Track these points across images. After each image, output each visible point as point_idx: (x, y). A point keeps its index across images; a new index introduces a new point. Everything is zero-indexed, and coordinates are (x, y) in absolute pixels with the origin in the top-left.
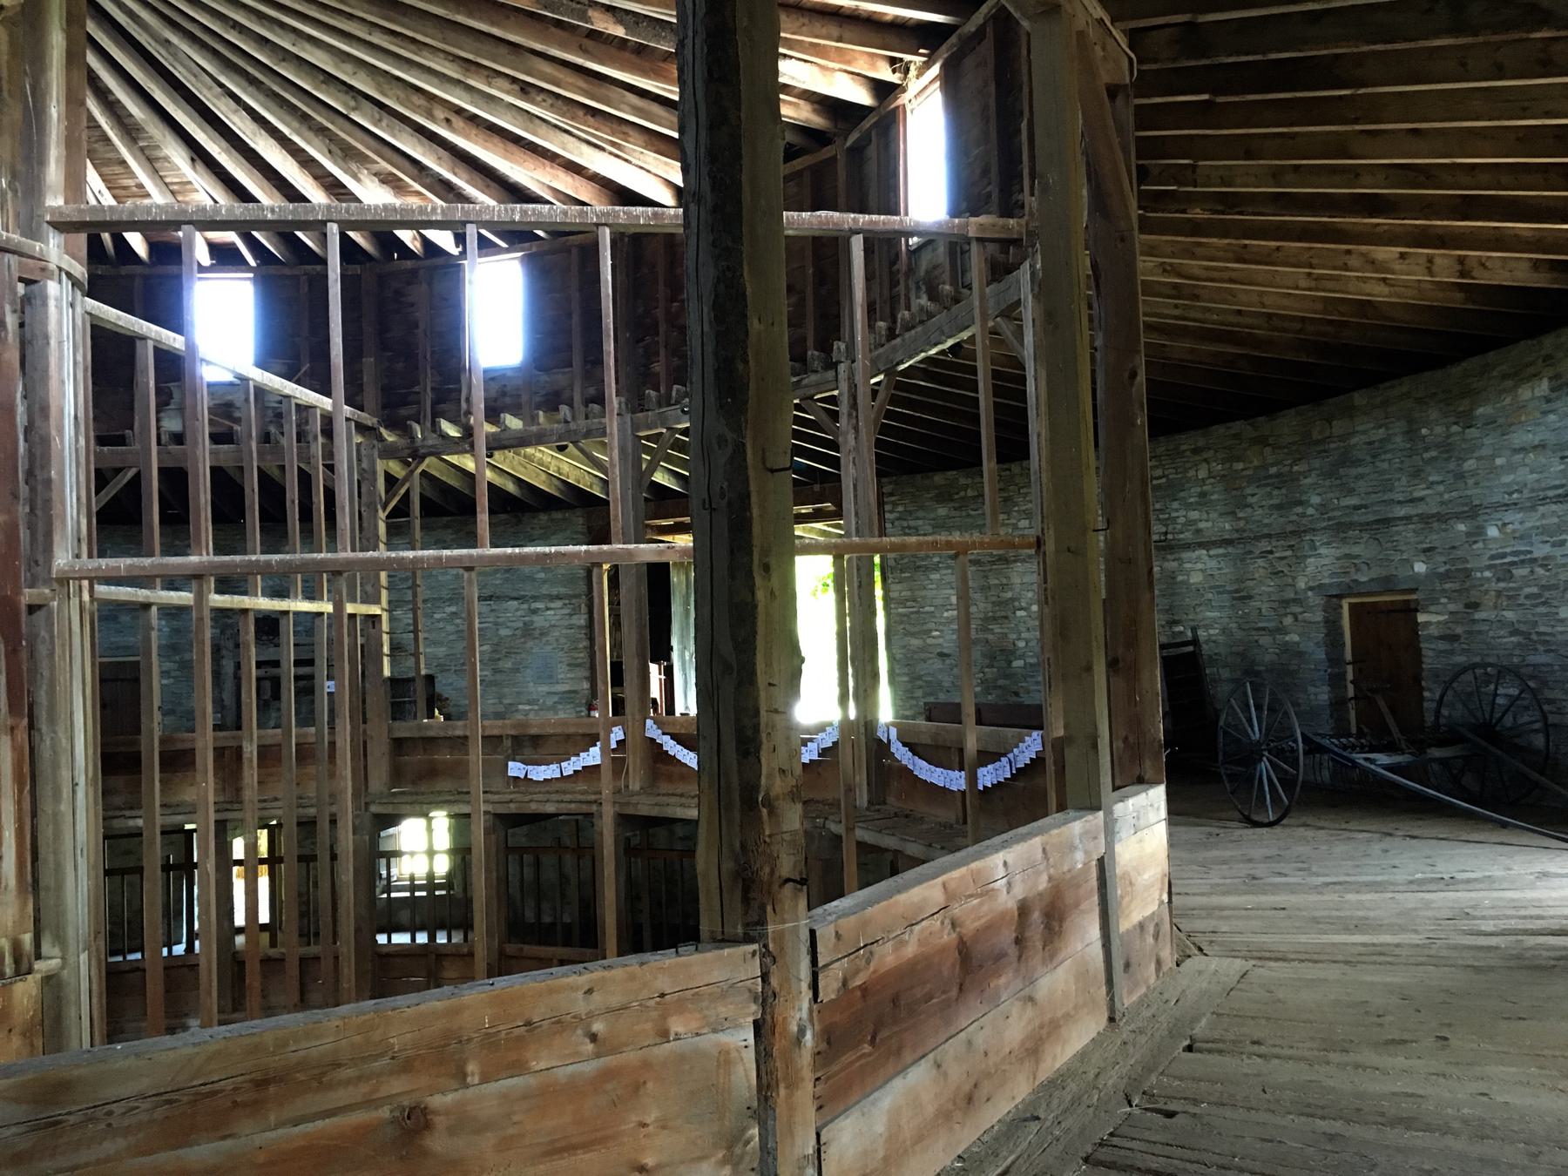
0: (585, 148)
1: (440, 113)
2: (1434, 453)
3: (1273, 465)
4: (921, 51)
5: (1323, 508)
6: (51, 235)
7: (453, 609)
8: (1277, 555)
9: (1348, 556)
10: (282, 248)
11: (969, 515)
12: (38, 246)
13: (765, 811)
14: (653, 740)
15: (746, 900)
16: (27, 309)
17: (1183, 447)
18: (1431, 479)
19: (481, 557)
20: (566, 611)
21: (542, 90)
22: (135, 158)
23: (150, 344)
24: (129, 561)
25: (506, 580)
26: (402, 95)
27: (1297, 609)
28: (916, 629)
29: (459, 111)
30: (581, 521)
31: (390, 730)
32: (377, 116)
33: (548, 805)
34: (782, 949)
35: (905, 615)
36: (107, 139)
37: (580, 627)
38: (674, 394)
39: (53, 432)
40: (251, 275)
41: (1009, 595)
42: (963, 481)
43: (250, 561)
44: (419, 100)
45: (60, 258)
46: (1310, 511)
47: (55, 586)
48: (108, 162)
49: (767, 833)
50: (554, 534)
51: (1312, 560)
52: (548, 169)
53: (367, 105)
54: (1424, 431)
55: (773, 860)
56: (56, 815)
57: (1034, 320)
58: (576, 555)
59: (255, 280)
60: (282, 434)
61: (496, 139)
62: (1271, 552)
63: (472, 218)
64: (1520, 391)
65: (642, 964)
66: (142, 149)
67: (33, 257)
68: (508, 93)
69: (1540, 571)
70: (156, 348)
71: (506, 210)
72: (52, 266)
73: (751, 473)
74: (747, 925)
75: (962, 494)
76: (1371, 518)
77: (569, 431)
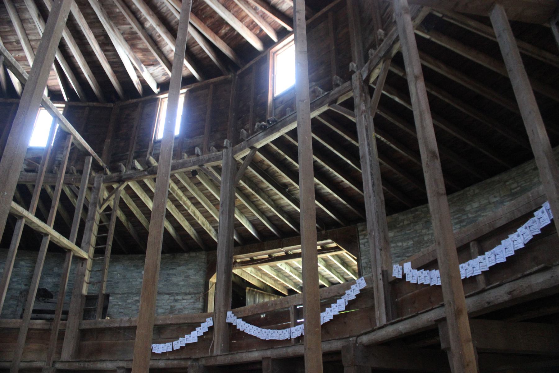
7: (137, 298)
10: (80, 91)
11: (406, 234)
14: (230, 324)
17: (527, 170)
20: (192, 301)
25: (165, 285)
30: (204, 257)
31: (80, 324)
33: (160, 362)
37: (198, 309)
38: (256, 126)
40: (64, 105)
42: (401, 218)
50: (190, 263)
75: (401, 224)
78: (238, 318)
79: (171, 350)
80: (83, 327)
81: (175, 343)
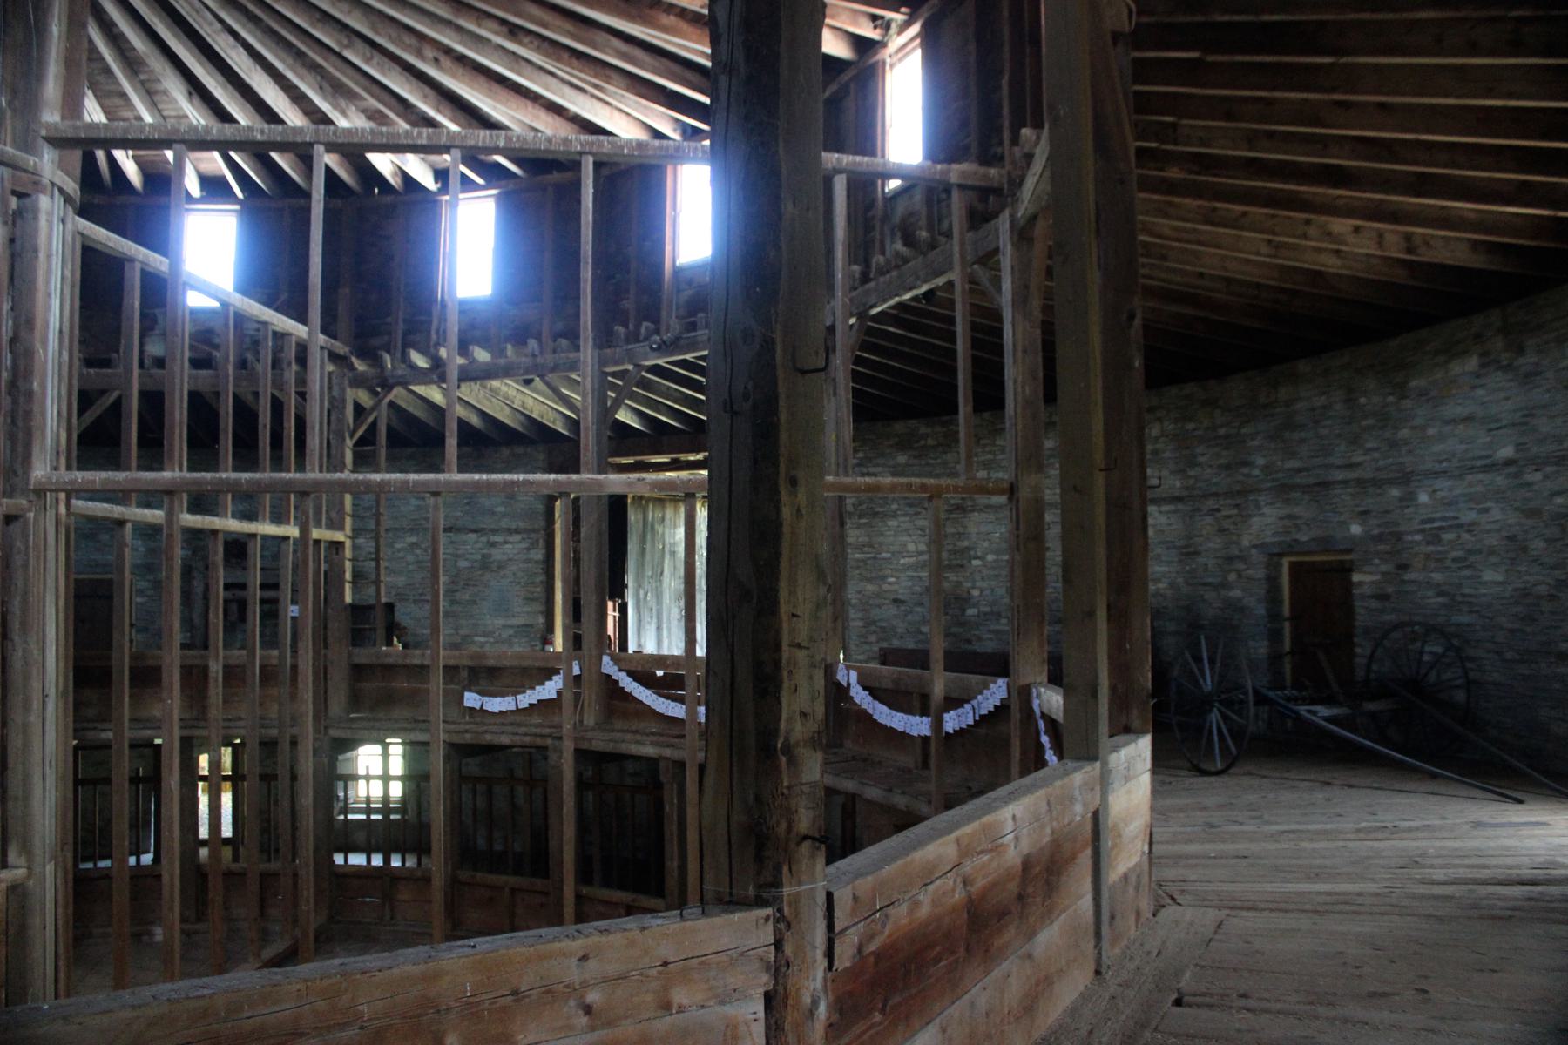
0: (567, 90)
1: (429, 52)
2: (1370, 422)
3: (1221, 426)
4: (903, 10)
5: (1267, 469)
6: (45, 151)
7: (414, 539)
8: (1224, 513)
9: (1289, 517)
11: (928, 464)
12: (32, 160)
13: (783, 759)
14: (609, 676)
15: (759, 859)
16: (19, 222)
18: (1369, 445)
19: (448, 483)
21: (529, 32)
22: (135, 91)
23: (138, 266)
24: (104, 475)
26: (394, 35)
27: (1242, 566)
28: (873, 575)
29: (448, 51)
30: (542, 457)
31: (350, 655)
32: (368, 55)
34: (797, 914)
35: (863, 560)
36: (108, 71)
37: (537, 562)
38: (643, 330)
39: (38, 345)
40: (237, 207)
41: (966, 543)
42: (923, 430)
43: (221, 479)
44: (409, 39)
45: (54, 174)
46: (1256, 472)
47: (32, 497)
48: (109, 94)
49: (786, 784)
52: (530, 108)
53: (359, 44)
54: (1363, 400)
55: (790, 815)
56: (25, 727)
57: (1012, 268)
58: (545, 483)
59: (240, 213)
60: (258, 360)
61: (482, 79)
62: (1218, 510)
63: (457, 143)
64: (1451, 366)
65: (643, 929)
66: (143, 83)
67: (26, 171)
68: (496, 33)
69: (1467, 536)
70: (143, 271)
71: (491, 136)
72: (45, 181)
73: (780, 373)
74: (759, 887)
75: (923, 442)
76: (1312, 481)
77: (536, 365)
78: (620, 670)
79: (514, 708)
80: (357, 660)
81: (519, 697)
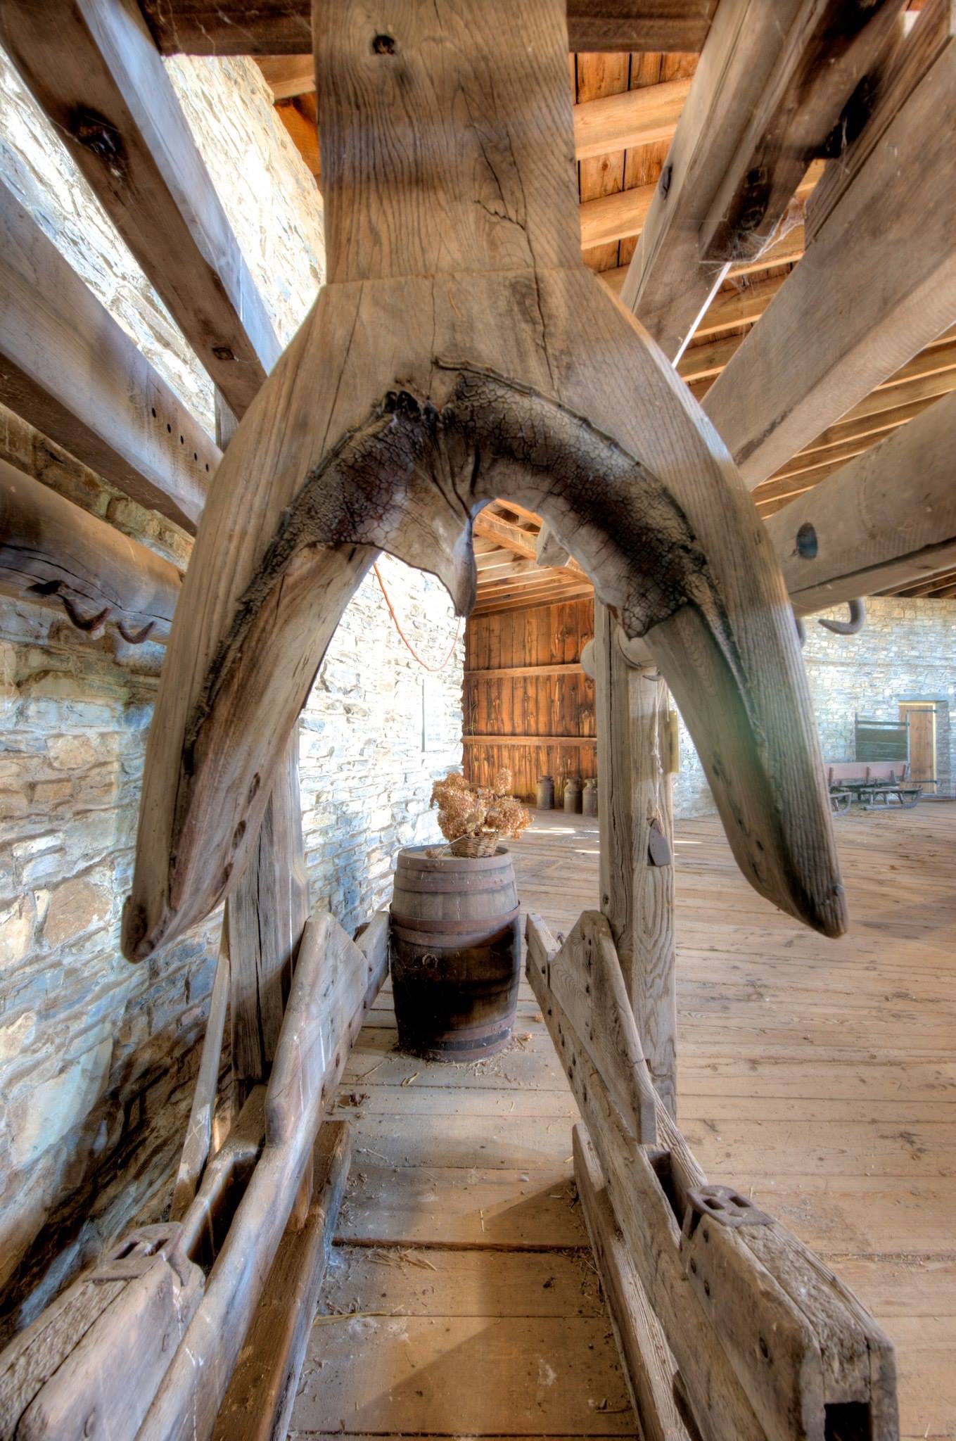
5: (899, 655)
27: (885, 707)
51: (895, 681)
76: (925, 664)
